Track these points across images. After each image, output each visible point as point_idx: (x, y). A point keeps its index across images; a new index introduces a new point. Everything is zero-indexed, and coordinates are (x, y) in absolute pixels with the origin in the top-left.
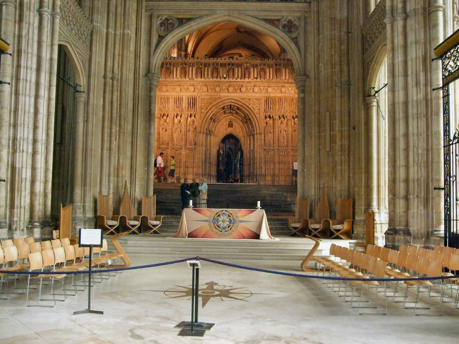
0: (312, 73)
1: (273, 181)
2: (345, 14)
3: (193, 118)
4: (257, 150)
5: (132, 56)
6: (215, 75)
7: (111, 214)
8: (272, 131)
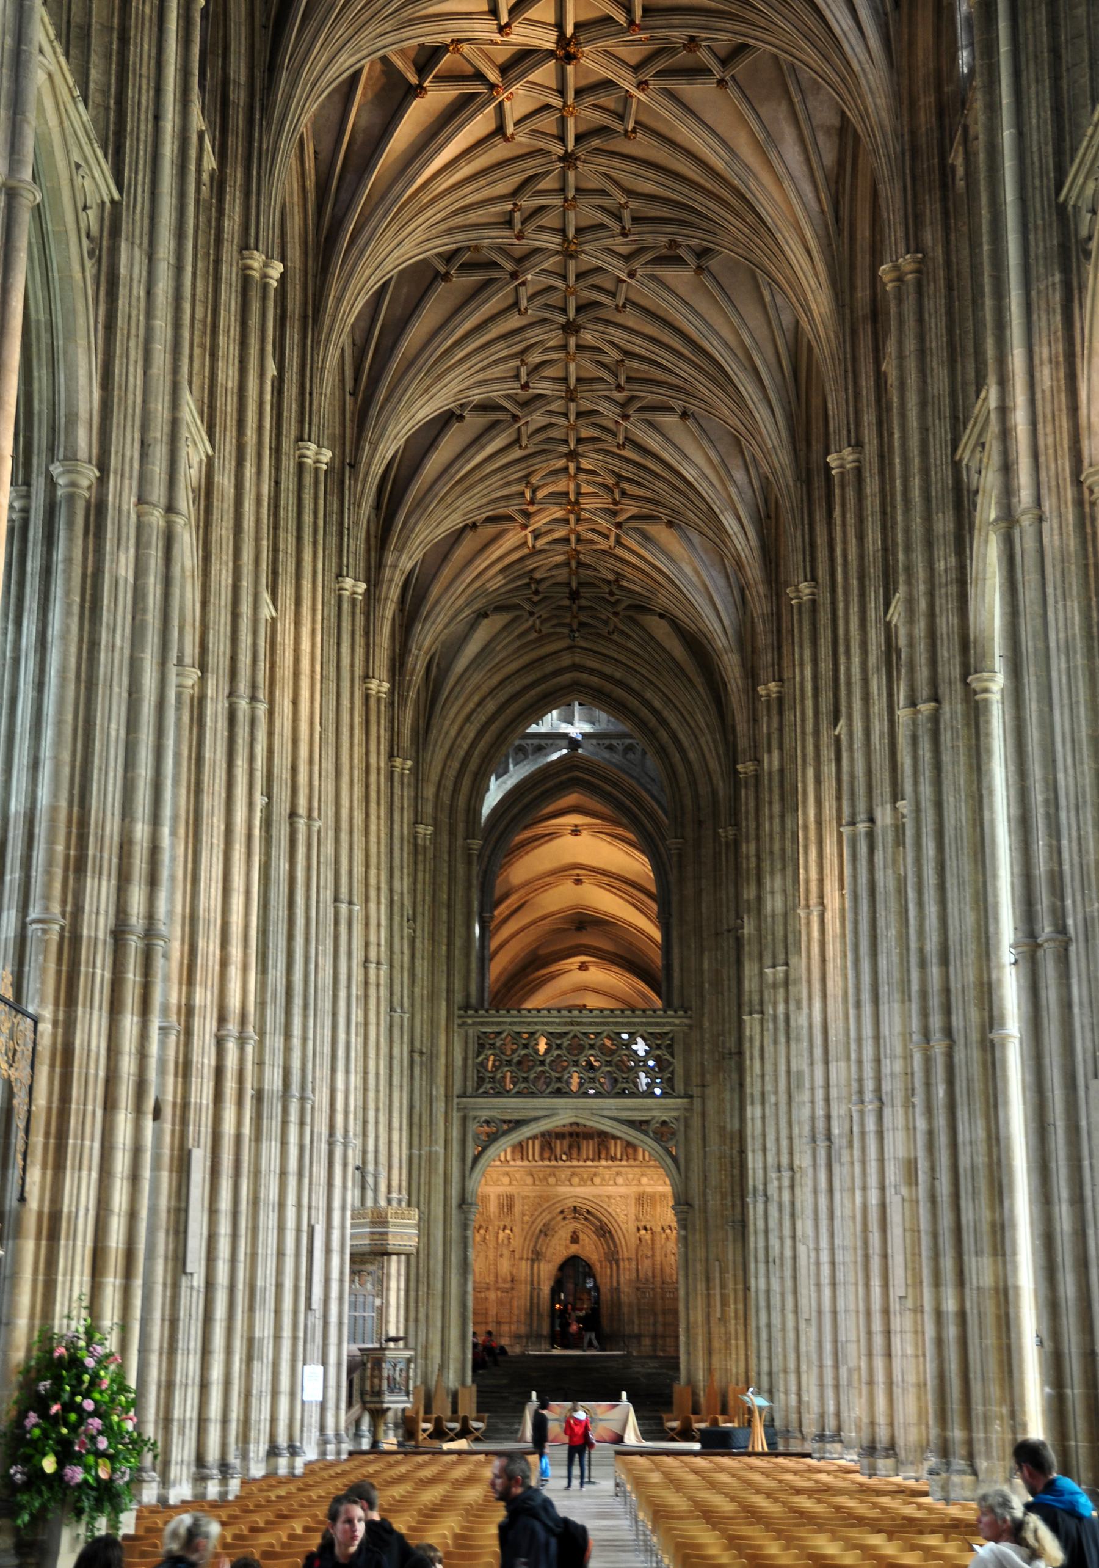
0: (696, 1202)
1: (654, 1346)
2: (737, 1126)
3: (508, 1231)
4: (625, 1288)
5: (441, 1180)
6: (546, 1155)
7: (449, 1414)
8: (650, 1254)
